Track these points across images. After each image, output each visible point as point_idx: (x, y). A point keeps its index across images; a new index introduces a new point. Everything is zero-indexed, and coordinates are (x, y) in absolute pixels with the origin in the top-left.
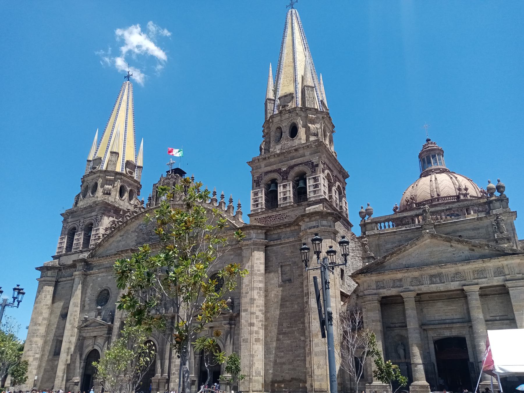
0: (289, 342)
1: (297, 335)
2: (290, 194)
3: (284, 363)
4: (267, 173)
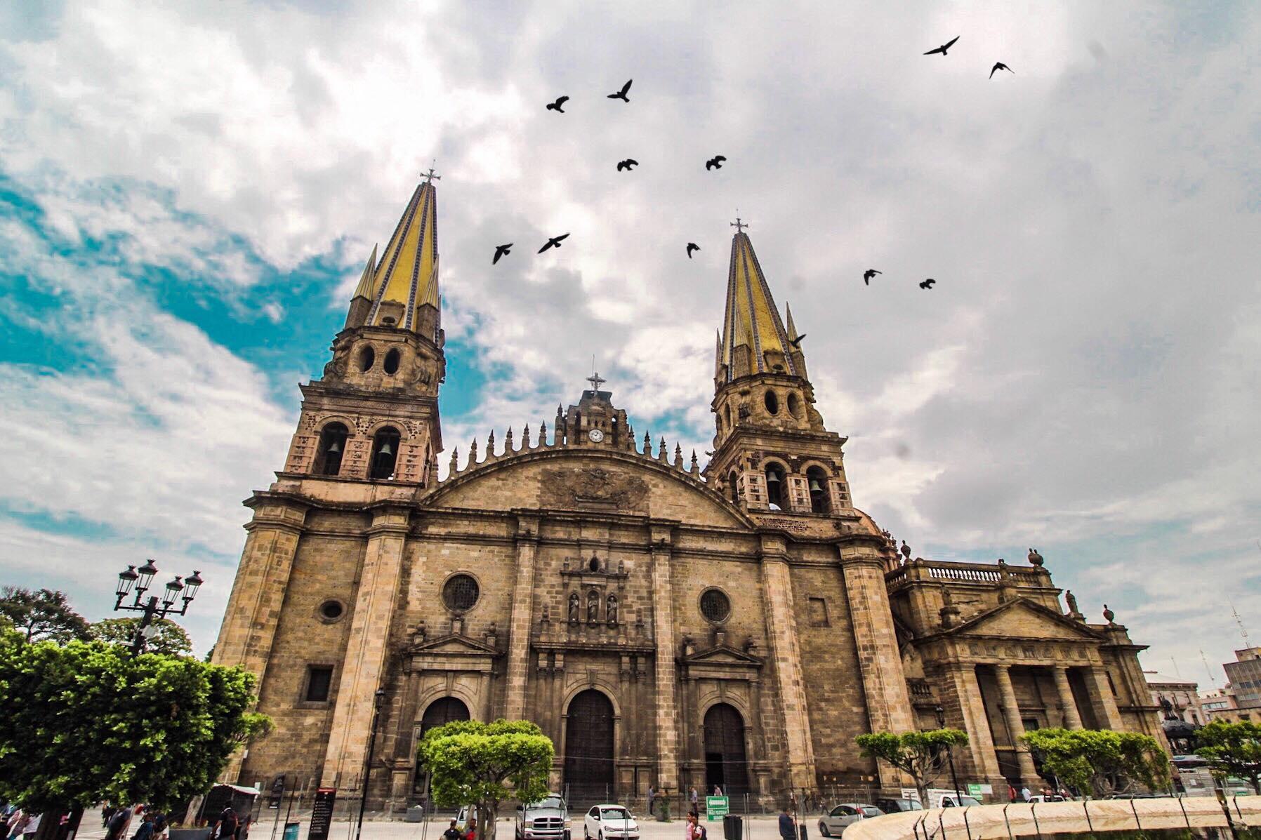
0: (836, 713)
1: (847, 704)
2: (806, 497)
3: (832, 746)
4: (767, 454)
